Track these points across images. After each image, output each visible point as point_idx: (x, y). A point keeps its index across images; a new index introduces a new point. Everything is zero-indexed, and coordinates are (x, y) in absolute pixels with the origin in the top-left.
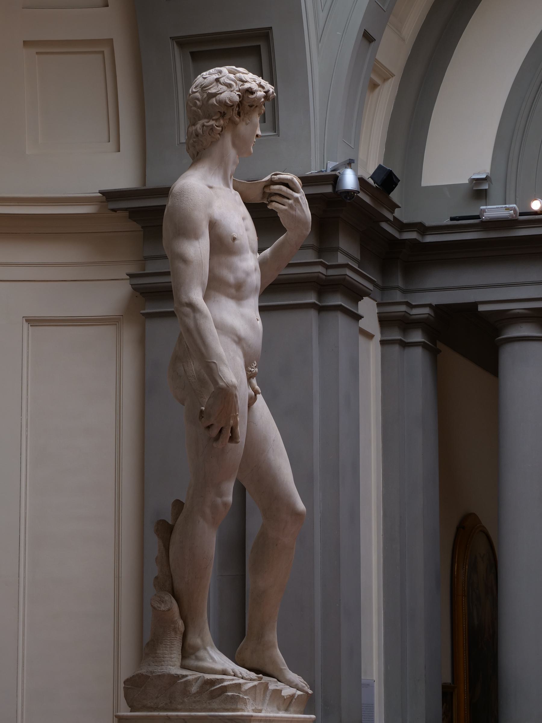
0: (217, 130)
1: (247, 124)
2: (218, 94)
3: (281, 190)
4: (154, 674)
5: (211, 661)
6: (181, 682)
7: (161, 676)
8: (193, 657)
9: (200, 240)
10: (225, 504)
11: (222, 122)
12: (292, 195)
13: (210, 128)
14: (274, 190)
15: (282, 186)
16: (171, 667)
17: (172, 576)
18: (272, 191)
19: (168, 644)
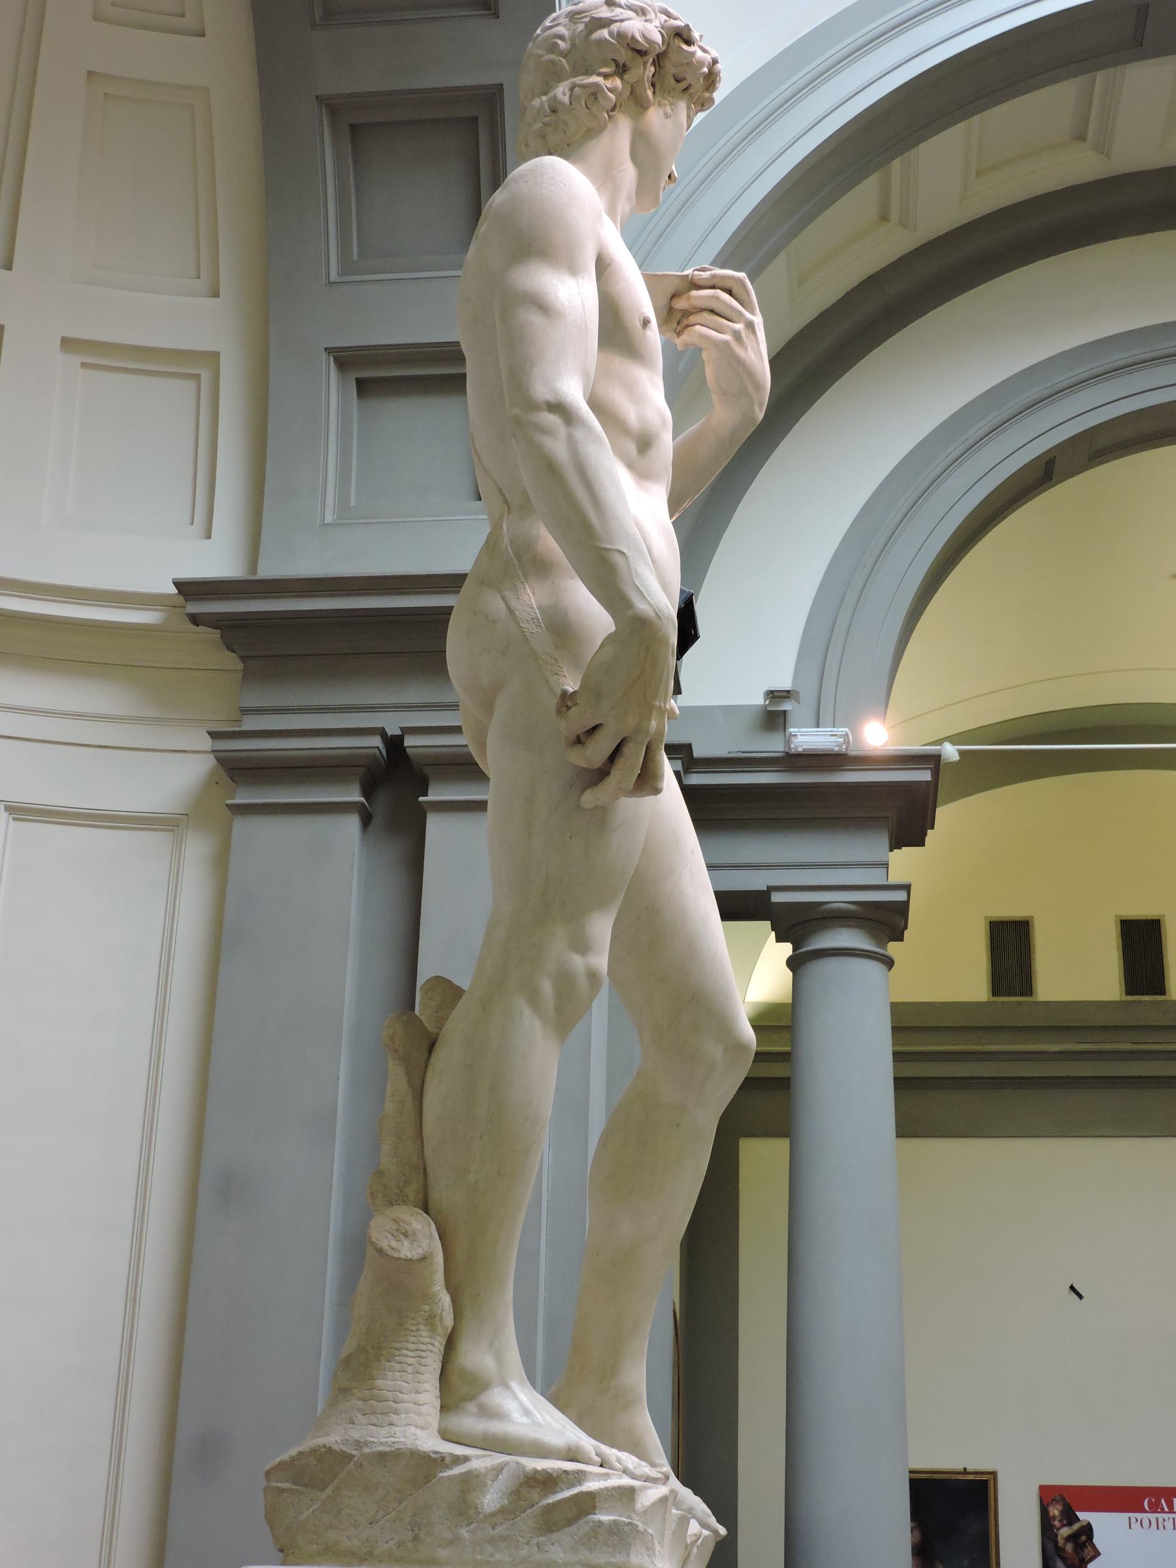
0: (606, 98)
1: (667, 116)
2: (616, 21)
3: (718, 298)
4: (367, 1450)
5: (525, 1420)
6: (450, 1478)
7: (384, 1458)
8: (472, 1407)
9: (580, 280)
10: (593, 976)
11: (618, 82)
12: (741, 314)
13: (592, 90)
14: (701, 297)
15: (719, 291)
16: (419, 1432)
17: (425, 1170)
18: (694, 302)
19: (410, 1360)
